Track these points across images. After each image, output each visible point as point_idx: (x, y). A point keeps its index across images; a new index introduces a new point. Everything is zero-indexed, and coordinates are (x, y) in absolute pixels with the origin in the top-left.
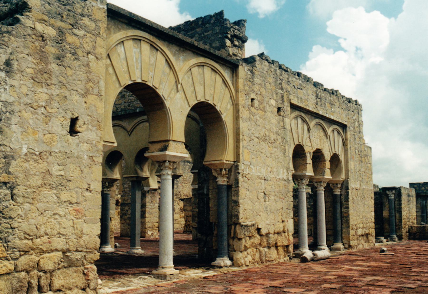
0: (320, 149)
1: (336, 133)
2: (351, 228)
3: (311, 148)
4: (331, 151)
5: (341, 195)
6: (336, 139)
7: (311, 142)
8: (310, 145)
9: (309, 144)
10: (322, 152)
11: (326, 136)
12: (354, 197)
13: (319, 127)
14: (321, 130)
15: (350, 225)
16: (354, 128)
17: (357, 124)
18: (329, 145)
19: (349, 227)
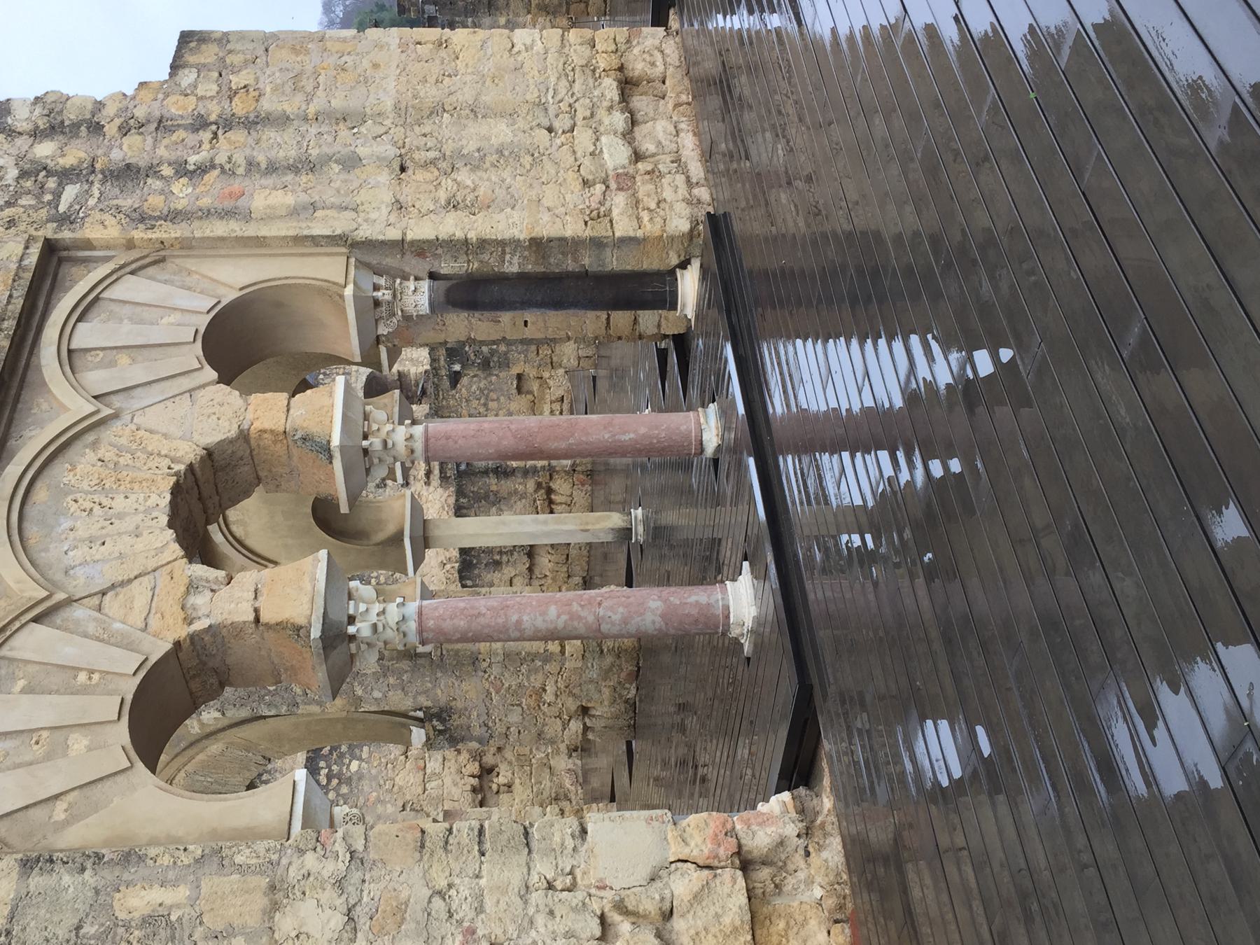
0: (176, 491)
1: (86, 335)
2: (601, 230)
3: (162, 577)
4: (186, 383)
5: (433, 276)
6: (126, 333)
7: (130, 581)
8: (151, 577)
9: (139, 591)
10: (191, 467)
11: (102, 422)
12: (442, 195)
13: (41, 494)
14: (61, 473)
15: (588, 233)
16: (66, 175)
17: (44, 150)
18: (155, 394)
19: (597, 244)
